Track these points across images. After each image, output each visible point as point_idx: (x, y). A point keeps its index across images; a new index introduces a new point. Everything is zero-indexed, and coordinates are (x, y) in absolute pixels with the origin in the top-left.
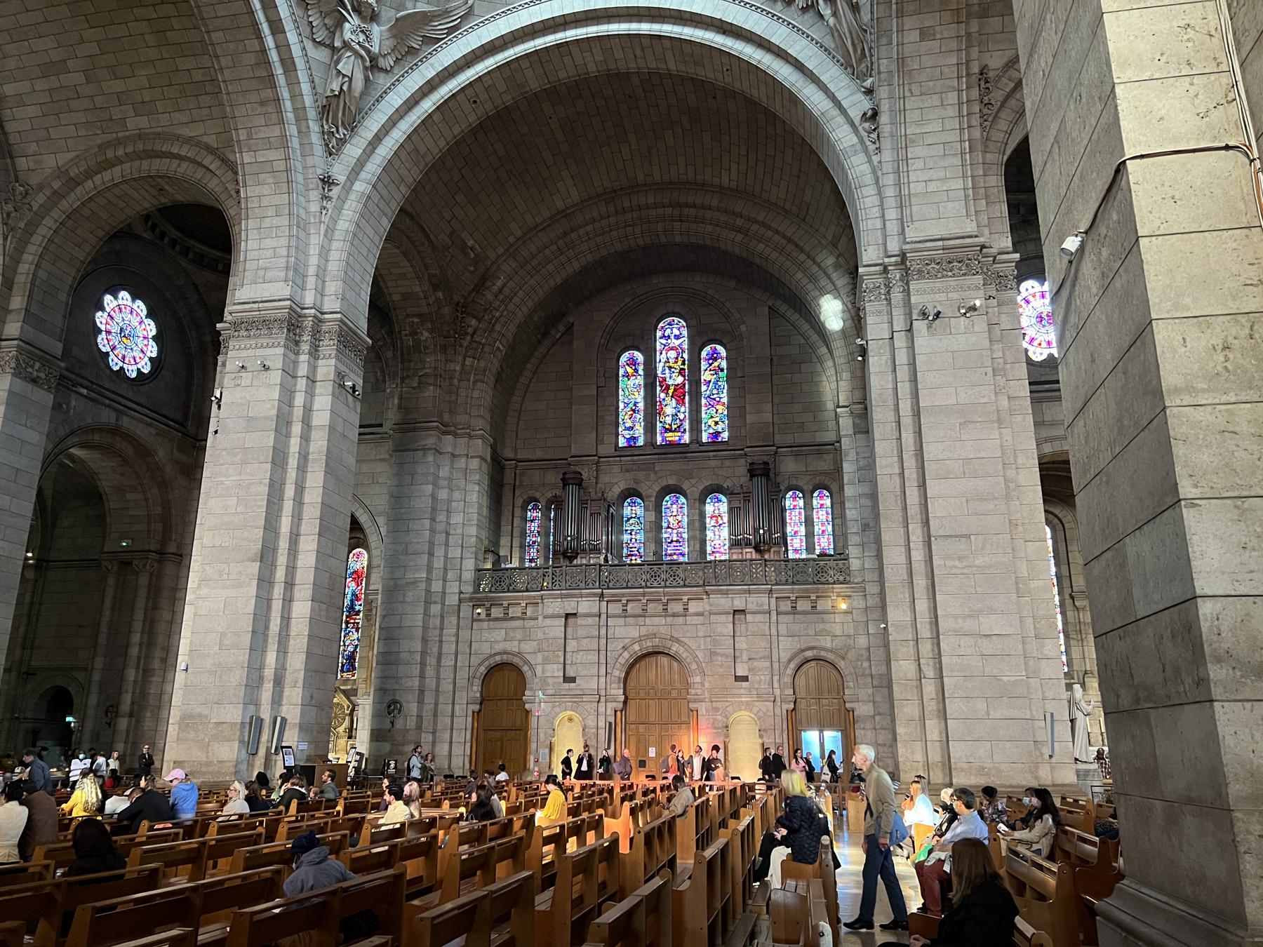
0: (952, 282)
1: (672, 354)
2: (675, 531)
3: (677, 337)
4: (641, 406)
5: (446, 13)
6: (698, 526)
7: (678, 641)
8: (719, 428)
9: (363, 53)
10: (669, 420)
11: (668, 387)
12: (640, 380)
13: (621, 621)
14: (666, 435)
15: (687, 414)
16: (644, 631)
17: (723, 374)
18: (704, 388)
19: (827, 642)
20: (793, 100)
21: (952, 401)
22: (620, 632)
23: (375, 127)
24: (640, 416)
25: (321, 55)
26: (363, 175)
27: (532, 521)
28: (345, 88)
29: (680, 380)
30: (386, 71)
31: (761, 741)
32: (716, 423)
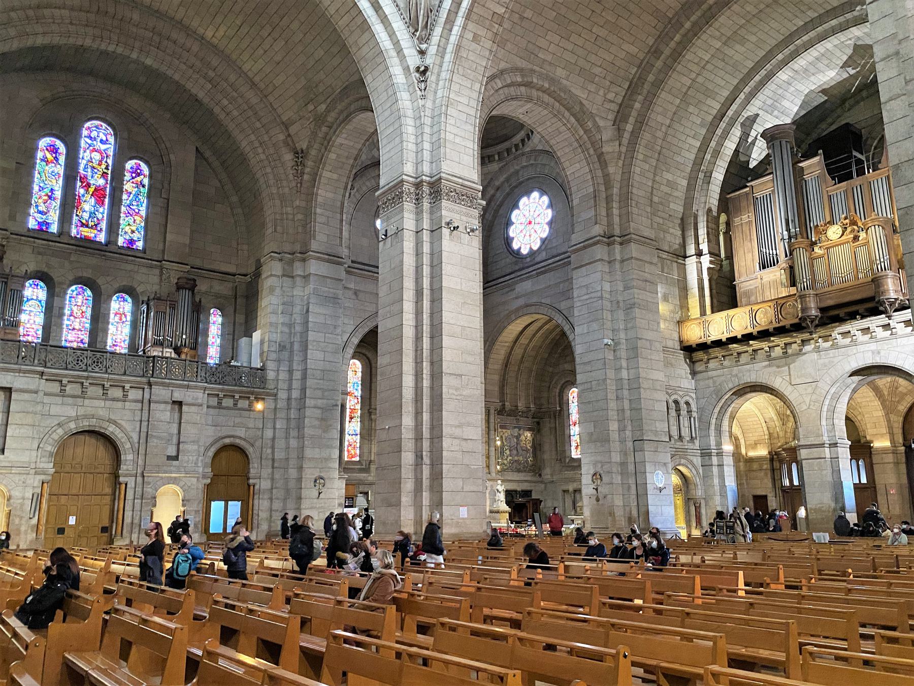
0: (464, 209)
1: (97, 156)
2: (78, 320)
4: (58, 194)
6: (99, 320)
7: (115, 423)
8: (135, 236)
10: (86, 216)
11: (89, 185)
12: (60, 169)
13: (59, 400)
14: (81, 229)
15: (105, 215)
16: (81, 411)
17: (145, 191)
18: (125, 197)
19: (241, 432)
20: (365, 26)
21: (459, 287)
22: (55, 410)
24: (57, 204)
29: (101, 182)
32: (133, 232)
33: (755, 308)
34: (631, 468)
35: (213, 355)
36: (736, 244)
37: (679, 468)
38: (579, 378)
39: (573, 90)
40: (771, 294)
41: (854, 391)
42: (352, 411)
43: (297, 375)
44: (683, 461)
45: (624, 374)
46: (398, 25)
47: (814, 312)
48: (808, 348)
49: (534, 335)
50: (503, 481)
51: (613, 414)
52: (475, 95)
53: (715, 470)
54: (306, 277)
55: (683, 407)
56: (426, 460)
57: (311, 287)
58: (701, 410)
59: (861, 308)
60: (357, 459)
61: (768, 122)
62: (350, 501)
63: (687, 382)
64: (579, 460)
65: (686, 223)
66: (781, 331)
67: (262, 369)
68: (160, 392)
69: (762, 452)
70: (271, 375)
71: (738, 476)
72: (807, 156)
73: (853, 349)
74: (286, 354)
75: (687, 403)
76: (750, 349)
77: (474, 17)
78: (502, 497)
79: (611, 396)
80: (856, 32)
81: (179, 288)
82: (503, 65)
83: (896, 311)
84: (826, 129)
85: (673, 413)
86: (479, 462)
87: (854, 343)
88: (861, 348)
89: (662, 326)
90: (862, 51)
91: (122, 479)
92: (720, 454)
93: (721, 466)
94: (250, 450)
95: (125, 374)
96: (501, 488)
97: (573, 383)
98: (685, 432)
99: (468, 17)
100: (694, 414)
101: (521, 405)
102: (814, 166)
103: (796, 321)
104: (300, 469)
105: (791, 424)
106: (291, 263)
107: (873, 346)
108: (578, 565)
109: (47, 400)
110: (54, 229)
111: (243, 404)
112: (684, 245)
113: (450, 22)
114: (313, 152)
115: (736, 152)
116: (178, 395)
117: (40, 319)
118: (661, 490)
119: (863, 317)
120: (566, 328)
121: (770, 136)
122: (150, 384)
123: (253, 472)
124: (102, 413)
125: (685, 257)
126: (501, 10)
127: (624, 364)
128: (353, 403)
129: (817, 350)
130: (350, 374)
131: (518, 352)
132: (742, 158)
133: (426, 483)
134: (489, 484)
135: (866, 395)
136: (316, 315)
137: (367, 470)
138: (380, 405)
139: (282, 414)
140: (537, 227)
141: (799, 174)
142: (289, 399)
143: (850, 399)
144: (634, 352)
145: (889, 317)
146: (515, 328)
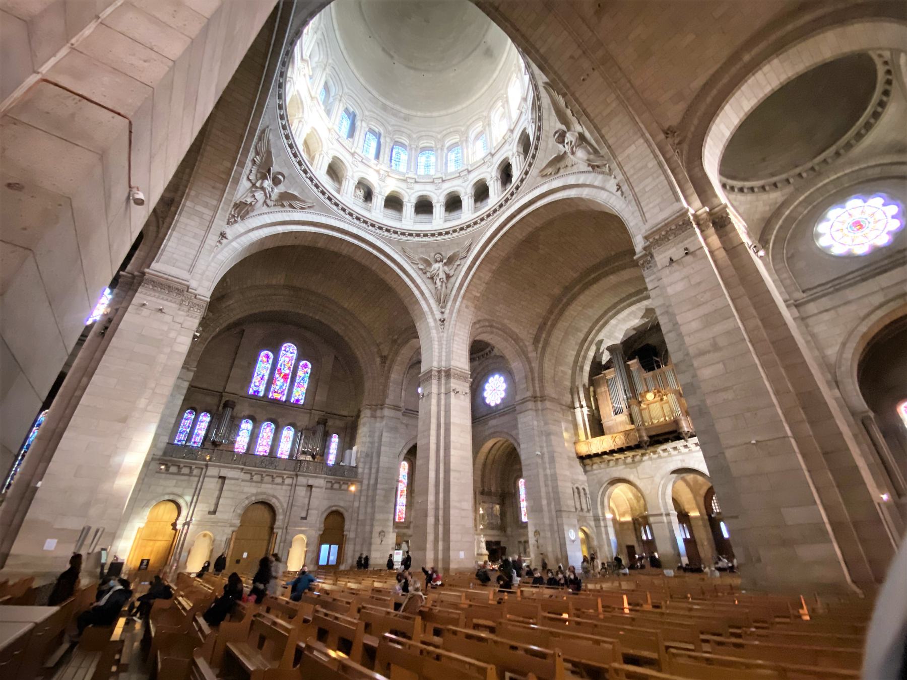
3: (291, 353)
4: (266, 377)
5: (304, 202)
9: (268, 195)
10: (277, 388)
12: (269, 366)
13: (248, 484)
16: (259, 490)
18: (297, 378)
19: (342, 504)
20: (417, 302)
22: (246, 489)
23: (254, 225)
25: (248, 185)
26: (238, 240)
27: (186, 419)
28: (253, 203)
30: (268, 206)
31: (305, 549)
33: (614, 435)
34: (556, 528)
35: (331, 459)
36: (600, 402)
37: (584, 528)
38: (524, 473)
39: (513, 329)
40: (622, 429)
41: (674, 483)
42: (402, 491)
43: (374, 471)
44: (585, 524)
45: (548, 472)
46: (432, 301)
47: (646, 438)
48: (645, 458)
49: (499, 449)
50: (485, 535)
51: (543, 494)
52: (467, 331)
53: (603, 529)
54: (382, 417)
55: (582, 491)
56: (441, 522)
57: (384, 422)
58: (592, 493)
59: (671, 436)
60: (403, 520)
61: (608, 343)
62: (398, 546)
63: (582, 477)
64: (526, 522)
65: (573, 391)
66: (629, 449)
67: (356, 467)
68: (302, 480)
69: (628, 518)
70: (360, 470)
71: (617, 534)
72: (630, 359)
73: (669, 459)
74: (369, 459)
75: (584, 489)
76: (614, 458)
77: (466, 298)
78: (483, 545)
79: (542, 484)
80: (646, 303)
81: (318, 423)
82: (479, 318)
83: (689, 437)
84: (638, 346)
85: (576, 495)
86: (470, 523)
87: (670, 455)
88: (674, 458)
89: (566, 445)
90: (649, 312)
91: (275, 531)
92: (605, 519)
93: (606, 527)
94: (346, 515)
95: (285, 470)
96: (483, 539)
97: (521, 476)
98: (584, 506)
99: (464, 297)
100: (588, 496)
101: (493, 489)
102: (634, 363)
103: (637, 443)
104: (372, 525)
105: (642, 502)
106: (375, 410)
107: (680, 457)
108: (529, 590)
109: (243, 483)
110: (261, 394)
111: (344, 487)
112: (573, 402)
113: (455, 300)
114: (390, 357)
115: (595, 357)
116: (311, 482)
117: (247, 440)
118: (573, 541)
119: (673, 441)
120: (516, 445)
121: (610, 349)
122: (297, 476)
123: (347, 526)
124: (271, 492)
125: (574, 408)
126: (478, 295)
127: (547, 466)
128: (402, 487)
129: (651, 459)
130: (401, 470)
131: (491, 457)
132: (598, 360)
133: (441, 536)
134: (476, 537)
135: (681, 485)
136: (386, 437)
137: (408, 527)
138: (416, 488)
139: (364, 493)
140: (498, 392)
141: (628, 368)
142: (369, 485)
143: (673, 487)
144: (552, 460)
145: (687, 441)
146: (490, 444)
